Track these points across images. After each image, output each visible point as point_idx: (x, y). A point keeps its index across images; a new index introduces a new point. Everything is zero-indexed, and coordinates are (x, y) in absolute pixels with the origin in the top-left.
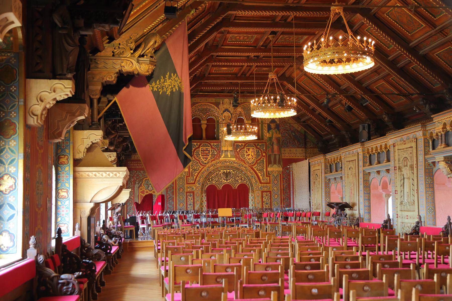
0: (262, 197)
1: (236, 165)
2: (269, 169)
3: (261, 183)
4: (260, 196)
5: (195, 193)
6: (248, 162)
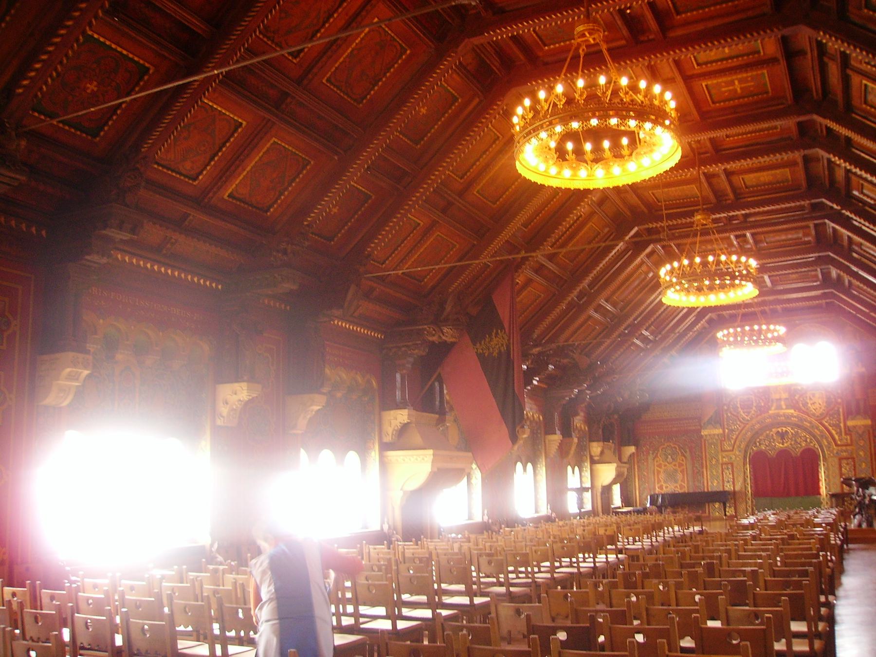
0: (840, 467)
2: (850, 423)
3: (837, 445)
4: (837, 466)
5: (735, 465)
6: (814, 415)
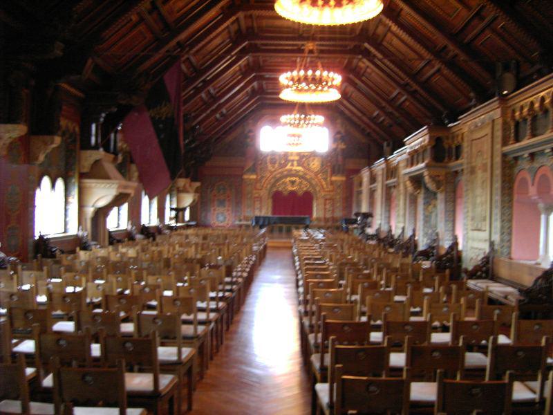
1: (301, 174)
